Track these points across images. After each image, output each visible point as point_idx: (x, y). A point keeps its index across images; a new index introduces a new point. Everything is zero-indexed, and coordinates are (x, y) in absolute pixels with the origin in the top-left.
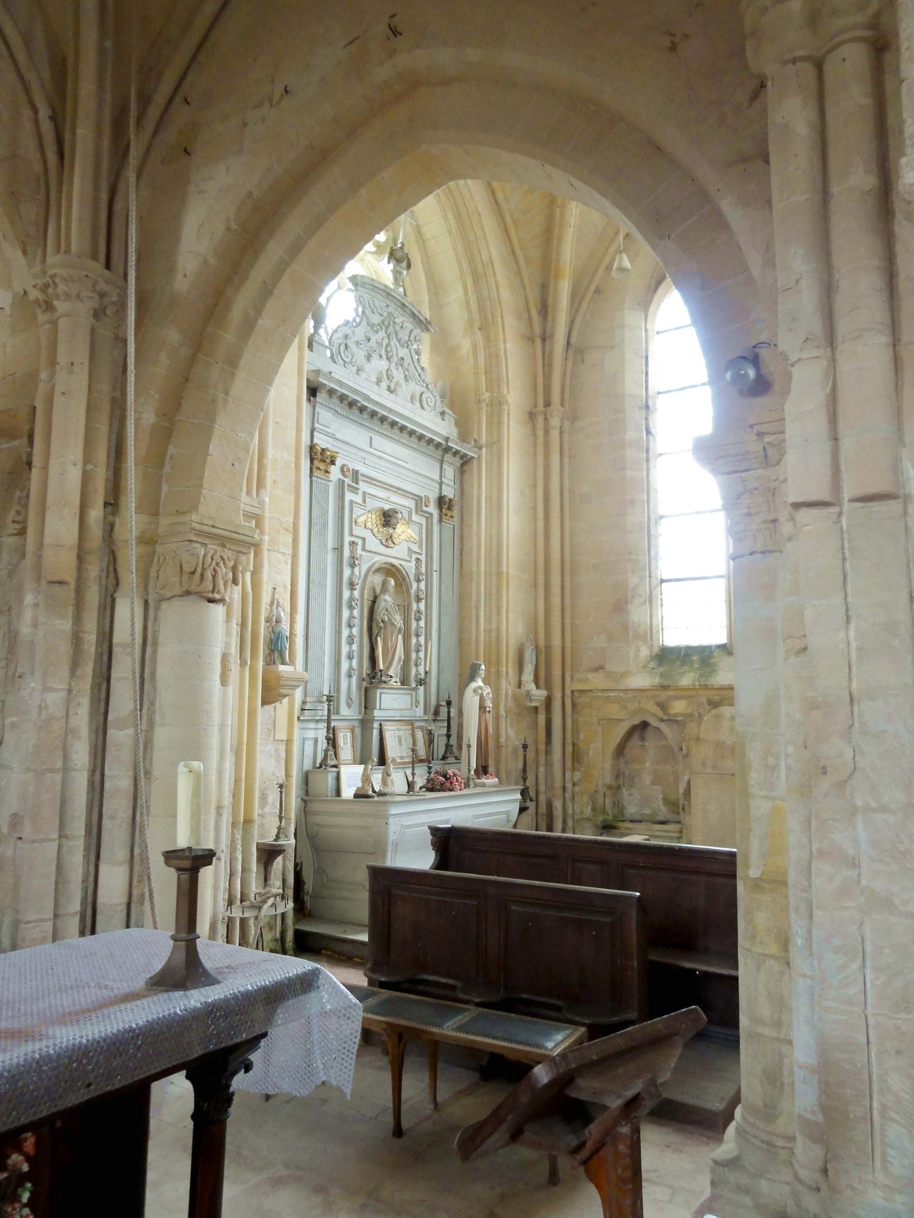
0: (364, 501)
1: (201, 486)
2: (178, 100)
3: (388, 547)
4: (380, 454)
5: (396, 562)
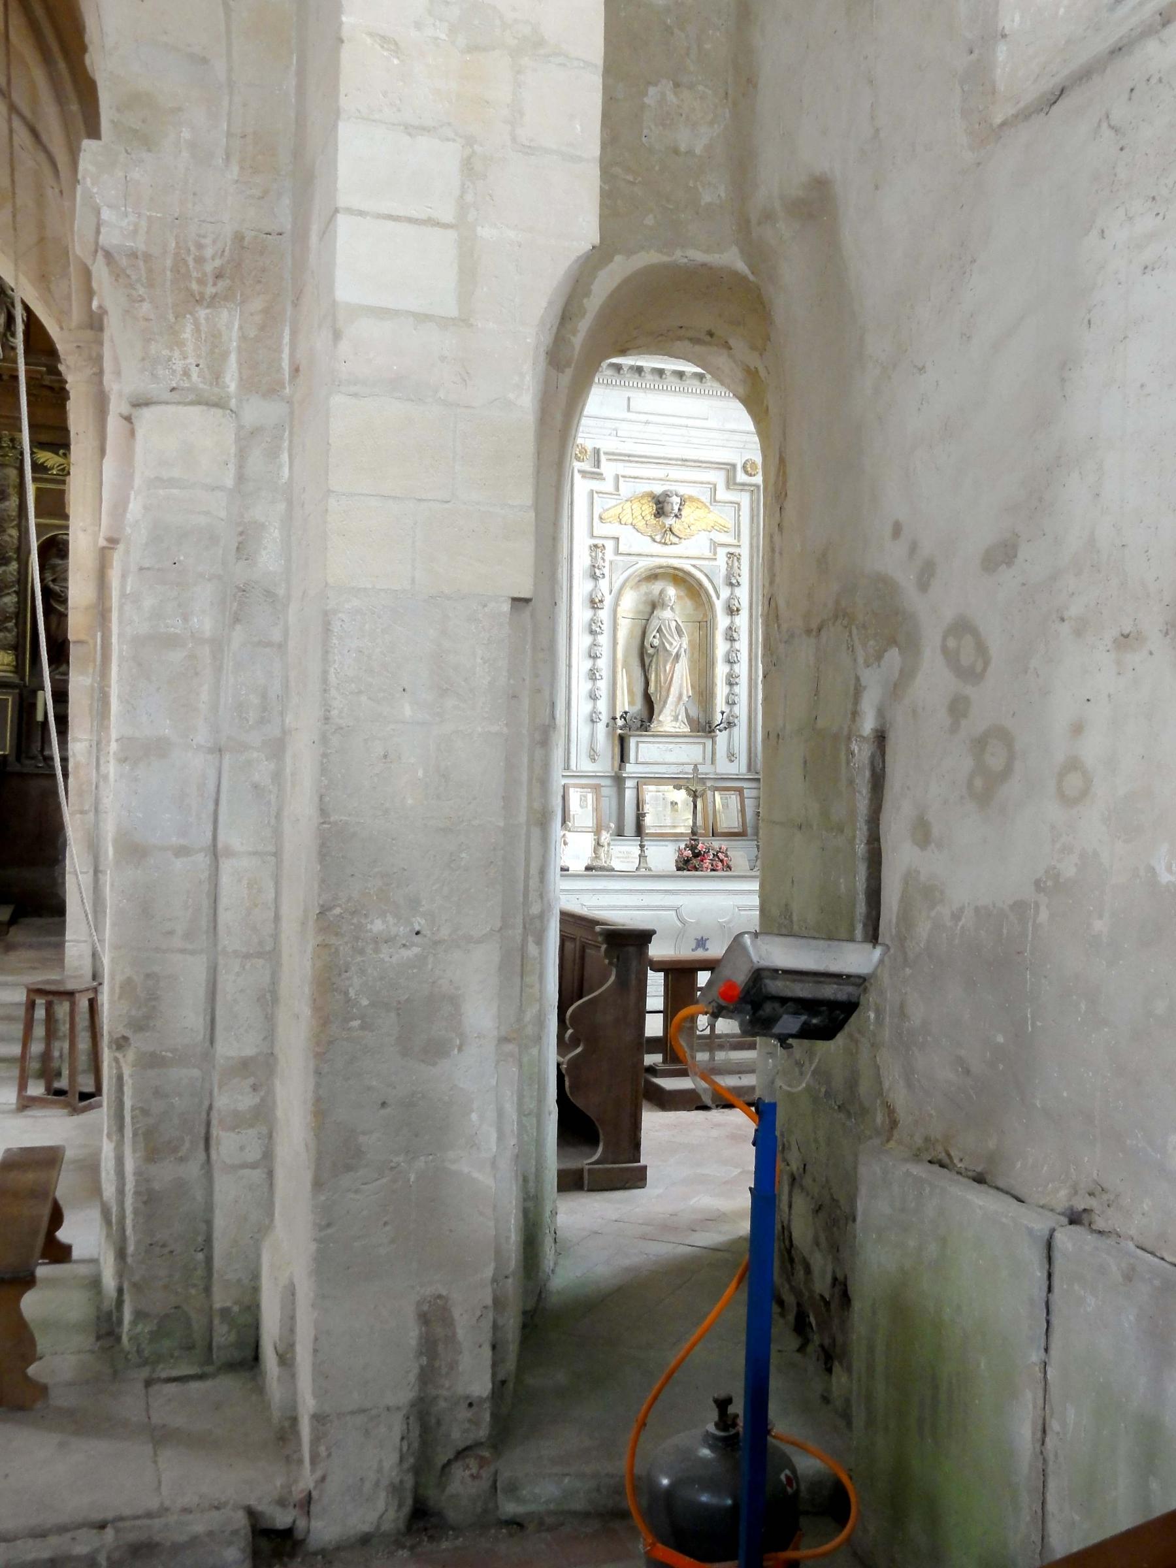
0: (617, 489)
3: (665, 544)
4: (644, 418)
5: (676, 563)
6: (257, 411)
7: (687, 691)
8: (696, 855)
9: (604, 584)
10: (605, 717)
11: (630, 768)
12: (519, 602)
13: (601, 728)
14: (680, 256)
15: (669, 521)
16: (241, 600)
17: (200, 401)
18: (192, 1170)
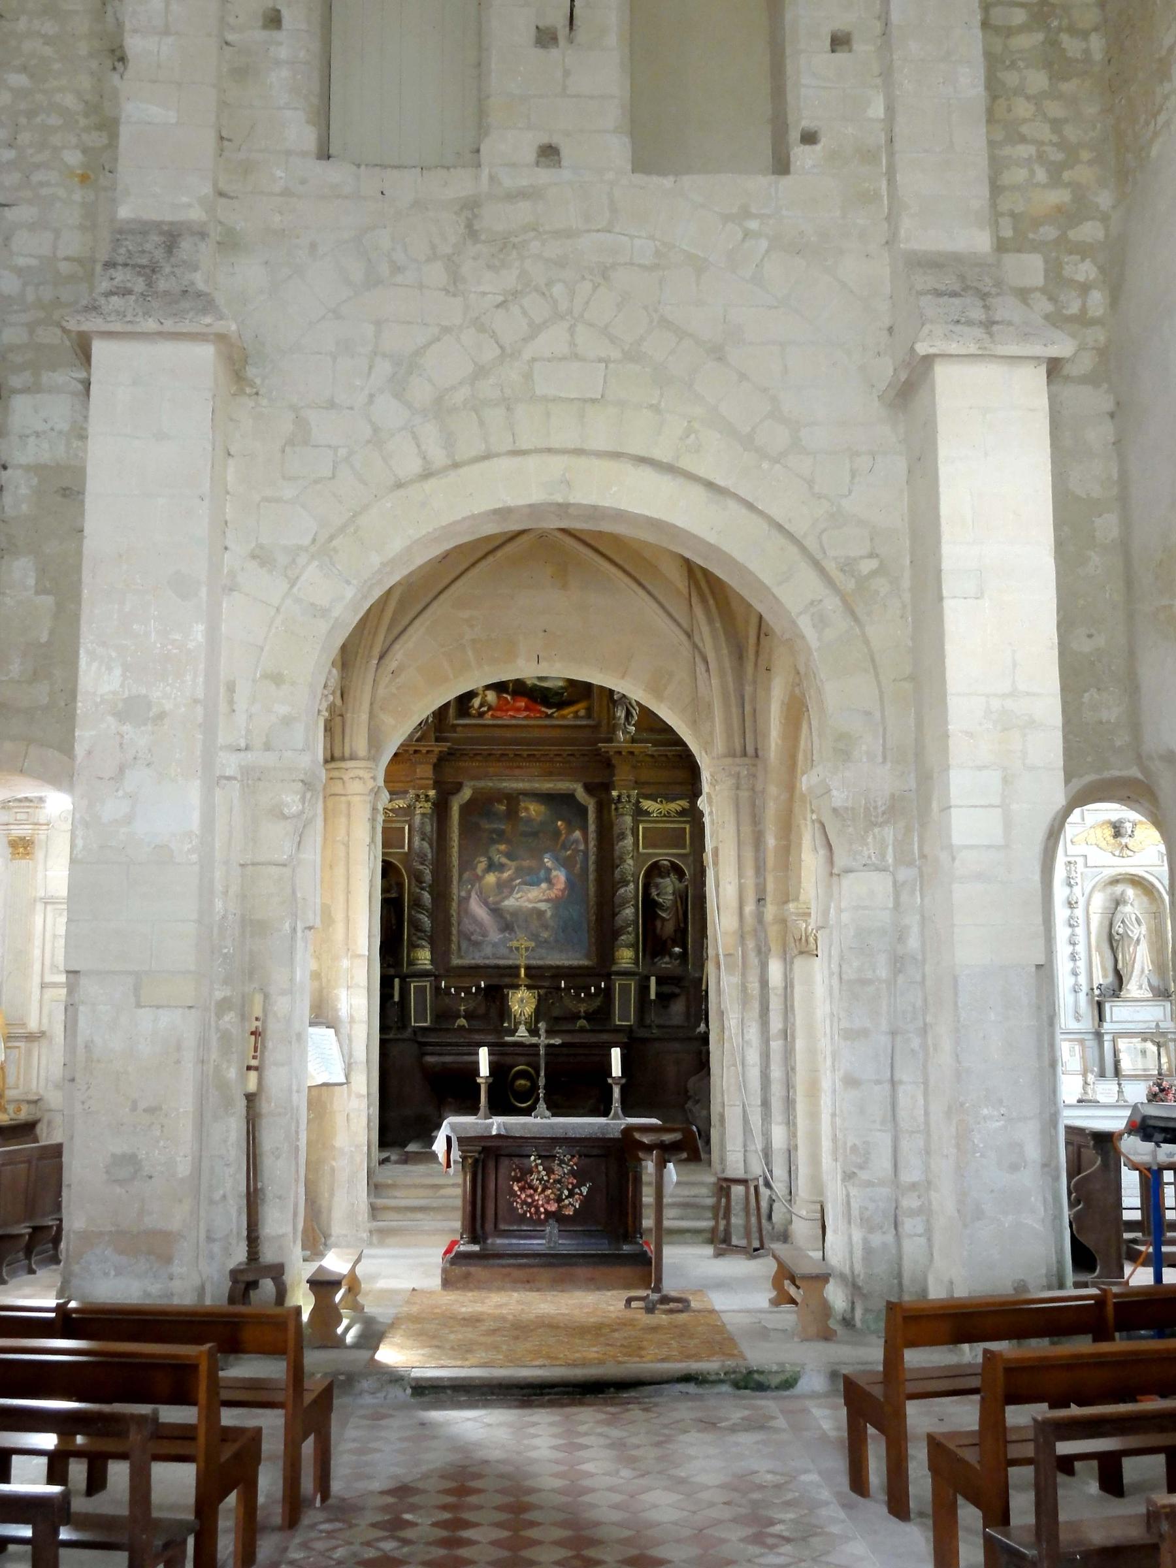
1: (800, 882)
2: (762, 635)
5: (1133, 871)
6: (904, 874)
7: (1148, 966)
8: (1162, 1090)
9: (1077, 890)
10: (1085, 988)
11: (1107, 1026)
12: (1039, 967)
13: (1082, 997)
14: (1107, 774)
15: (1124, 840)
16: (898, 963)
17: (877, 869)
18: (890, 1238)
